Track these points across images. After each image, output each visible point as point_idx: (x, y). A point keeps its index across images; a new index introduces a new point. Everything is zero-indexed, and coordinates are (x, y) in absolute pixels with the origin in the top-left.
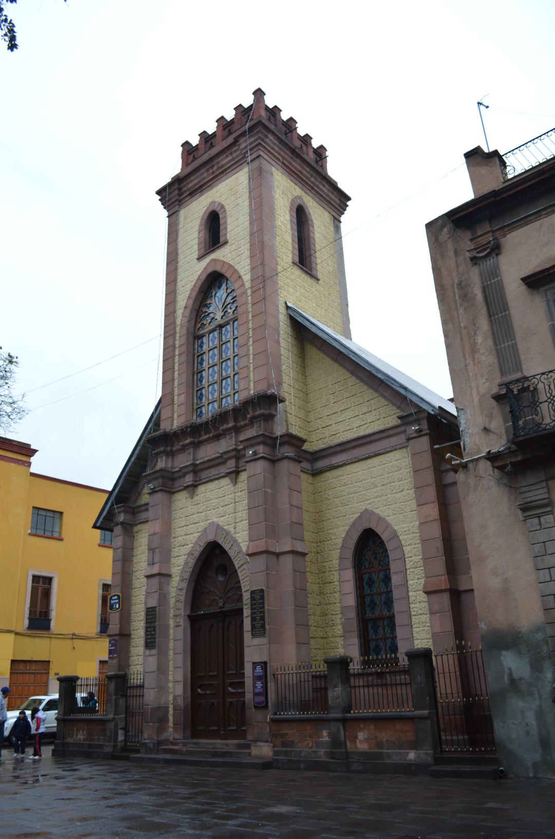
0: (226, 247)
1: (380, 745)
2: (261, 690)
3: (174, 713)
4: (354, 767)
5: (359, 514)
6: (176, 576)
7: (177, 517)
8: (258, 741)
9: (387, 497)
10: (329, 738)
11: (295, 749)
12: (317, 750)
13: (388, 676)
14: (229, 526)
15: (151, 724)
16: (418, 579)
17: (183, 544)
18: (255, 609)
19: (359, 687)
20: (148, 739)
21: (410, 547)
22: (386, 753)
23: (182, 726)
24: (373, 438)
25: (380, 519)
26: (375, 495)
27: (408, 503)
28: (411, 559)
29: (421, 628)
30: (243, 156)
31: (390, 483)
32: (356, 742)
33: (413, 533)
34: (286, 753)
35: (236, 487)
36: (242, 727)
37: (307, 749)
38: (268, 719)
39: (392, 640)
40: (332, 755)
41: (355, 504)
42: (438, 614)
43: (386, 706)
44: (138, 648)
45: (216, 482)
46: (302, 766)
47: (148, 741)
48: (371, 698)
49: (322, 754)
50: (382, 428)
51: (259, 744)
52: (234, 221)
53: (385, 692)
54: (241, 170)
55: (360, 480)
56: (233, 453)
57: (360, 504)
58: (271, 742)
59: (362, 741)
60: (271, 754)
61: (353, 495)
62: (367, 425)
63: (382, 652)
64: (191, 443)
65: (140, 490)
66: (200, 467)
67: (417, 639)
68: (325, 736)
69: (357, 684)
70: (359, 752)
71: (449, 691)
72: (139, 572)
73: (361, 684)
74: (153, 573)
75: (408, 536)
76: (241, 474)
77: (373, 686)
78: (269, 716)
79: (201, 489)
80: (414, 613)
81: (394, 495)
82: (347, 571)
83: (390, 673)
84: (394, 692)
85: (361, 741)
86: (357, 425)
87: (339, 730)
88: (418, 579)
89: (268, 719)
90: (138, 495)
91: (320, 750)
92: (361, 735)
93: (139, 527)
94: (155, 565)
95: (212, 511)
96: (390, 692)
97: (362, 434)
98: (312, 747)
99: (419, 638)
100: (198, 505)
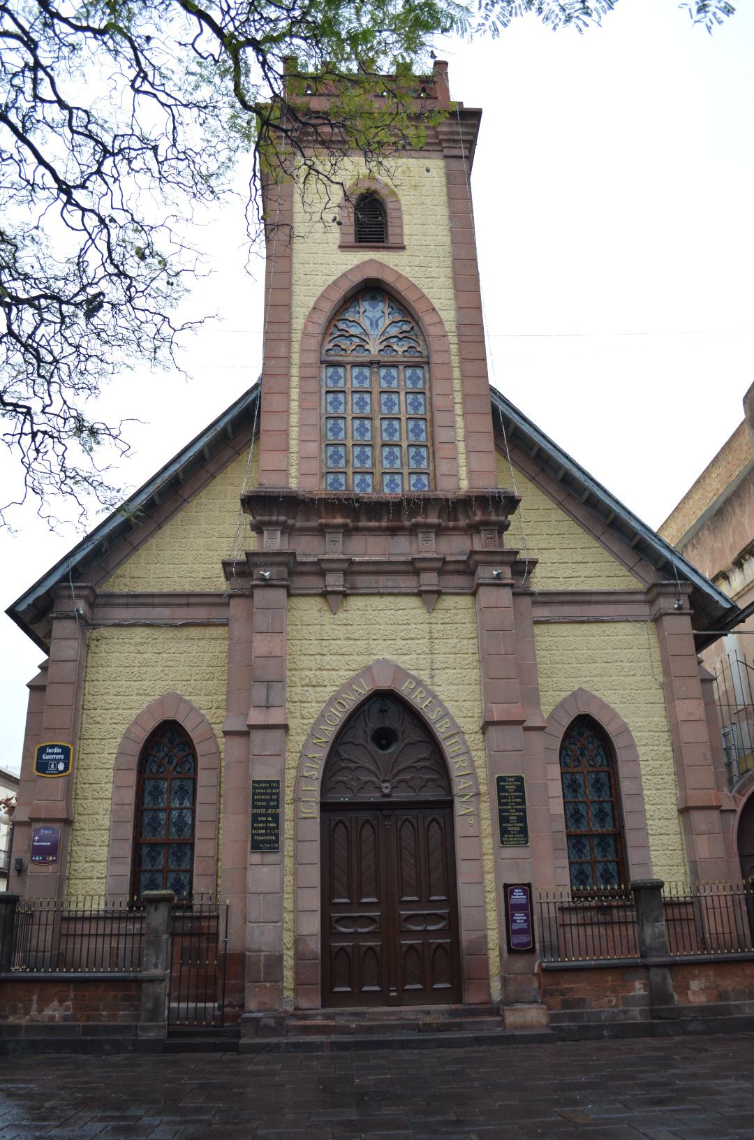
0: (401, 253)
1: (723, 995)
2: (525, 926)
3: (296, 965)
4: (691, 1027)
5: (569, 693)
6: (298, 734)
7: (298, 637)
8: (517, 1002)
9: (612, 678)
10: (645, 991)
11: (589, 1010)
12: (625, 1008)
13: (615, 911)
14: (421, 672)
15: (268, 984)
16: (658, 789)
17: (315, 683)
18: (507, 804)
19: (571, 925)
20: (259, 1011)
21: (646, 748)
22: (735, 1005)
23: (319, 987)
24: (594, 598)
25: (604, 706)
26: (595, 672)
27: (643, 692)
28: (647, 763)
29: (661, 852)
30: (437, 141)
31: (616, 661)
32: (687, 994)
33: (650, 731)
34: (573, 1017)
35: (432, 615)
36: (434, 984)
37: (607, 1009)
38: (536, 968)
39: (606, 865)
40: (653, 1014)
41: (563, 679)
42: (706, 836)
43: (611, 951)
44: (92, 848)
45: (391, 599)
46: (606, 1033)
47: (260, 1015)
48: (590, 941)
49: (636, 1014)
50: (604, 588)
51: (519, 1006)
52: (416, 224)
53: (609, 932)
54: (430, 158)
55: (572, 648)
56: (439, 565)
57: (571, 679)
58: (542, 1003)
59: (697, 992)
60: (544, 1021)
61: (560, 666)
62: (581, 579)
63: (590, 880)
64: (345, 526)
65: (110, 568)
66: (356, 568)
67: (656, 865)
68: (639, 989)
69: (567, 922)
70: (694, 1007)
71: (720, 930)
72: (99, 711)
73: (574, 921)
74: (270, 723)
75: (643, 733)
76: (444, 597)
77: (592, 924)
78: (536, 965)
79: (355, 603)
80: (652, 832)
81: (623, 678)
82: (553, 766)
83: (618, 907)
84: (624, 933)
85: (694, 993)
86: (565, 575)
87: (664, 979)
88: (658, 789)
89: (536, 968)
90: (105, 576)
91: (631, 1008)
92: (695, 985)
93: (104, 632)
94: (271, 710)
95: (380, 641)
96: (617, 933)
97: (572, 588)
98: (615, 1006)
99: (659, 864)
100: (349, 627)
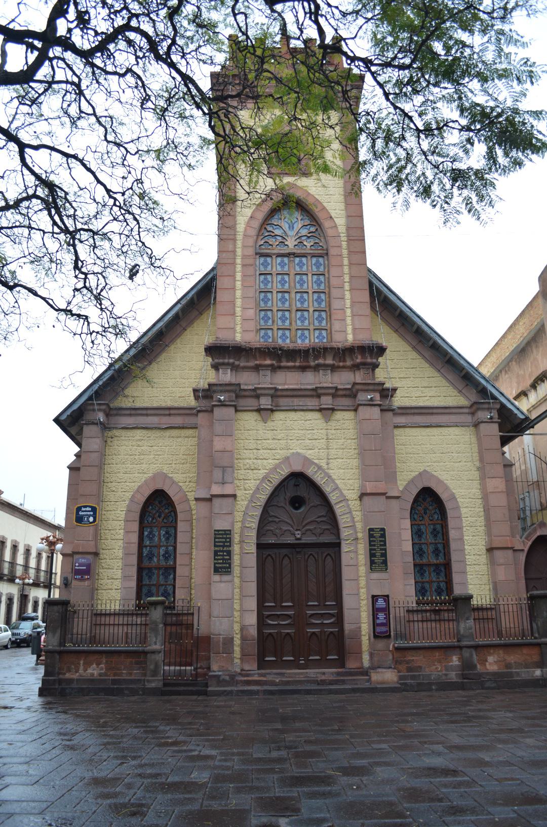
1: (508, 666)
2: (385, 621)
4: (488, 684)
5: (417, 473)
6: (242, 500)
7: (242, 437)
8: (379, 667)
20: (219, 671)
23: (256, 657)
24: (435, 411)
25: (440, 481)
32: (485, 665)
33: (470, 498)
34: (413, 677)
36: (327, 656)
38: (391, 647)
40: (464, 676)
43: (443, 637)
45: (302, 413)
46: (434, 687)
47: (220, 673)
48: (425, 632)
49: (453, 676)
50: (442, 404)
51: (380, 670)
53: (438, 626)
56: (333, 391)
58: (394, 668)
59: (492, 663)
60: (395, 679)
63: (428, 593)
64: (272, 365)
66: (279, 393)
68: (455, 660)
69: (411, 619)
71: (512, 626)
76: (336, 412)
77: (431, 621)
79: (279, 416)
85: (490, 664)
87: (471, 656)
90: (115, 396)
92: (491, 659)
93: (116, 432)
95: (295, 441)
97: (421, 404)
98: (441, 671)
100: (275, 432)
